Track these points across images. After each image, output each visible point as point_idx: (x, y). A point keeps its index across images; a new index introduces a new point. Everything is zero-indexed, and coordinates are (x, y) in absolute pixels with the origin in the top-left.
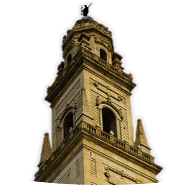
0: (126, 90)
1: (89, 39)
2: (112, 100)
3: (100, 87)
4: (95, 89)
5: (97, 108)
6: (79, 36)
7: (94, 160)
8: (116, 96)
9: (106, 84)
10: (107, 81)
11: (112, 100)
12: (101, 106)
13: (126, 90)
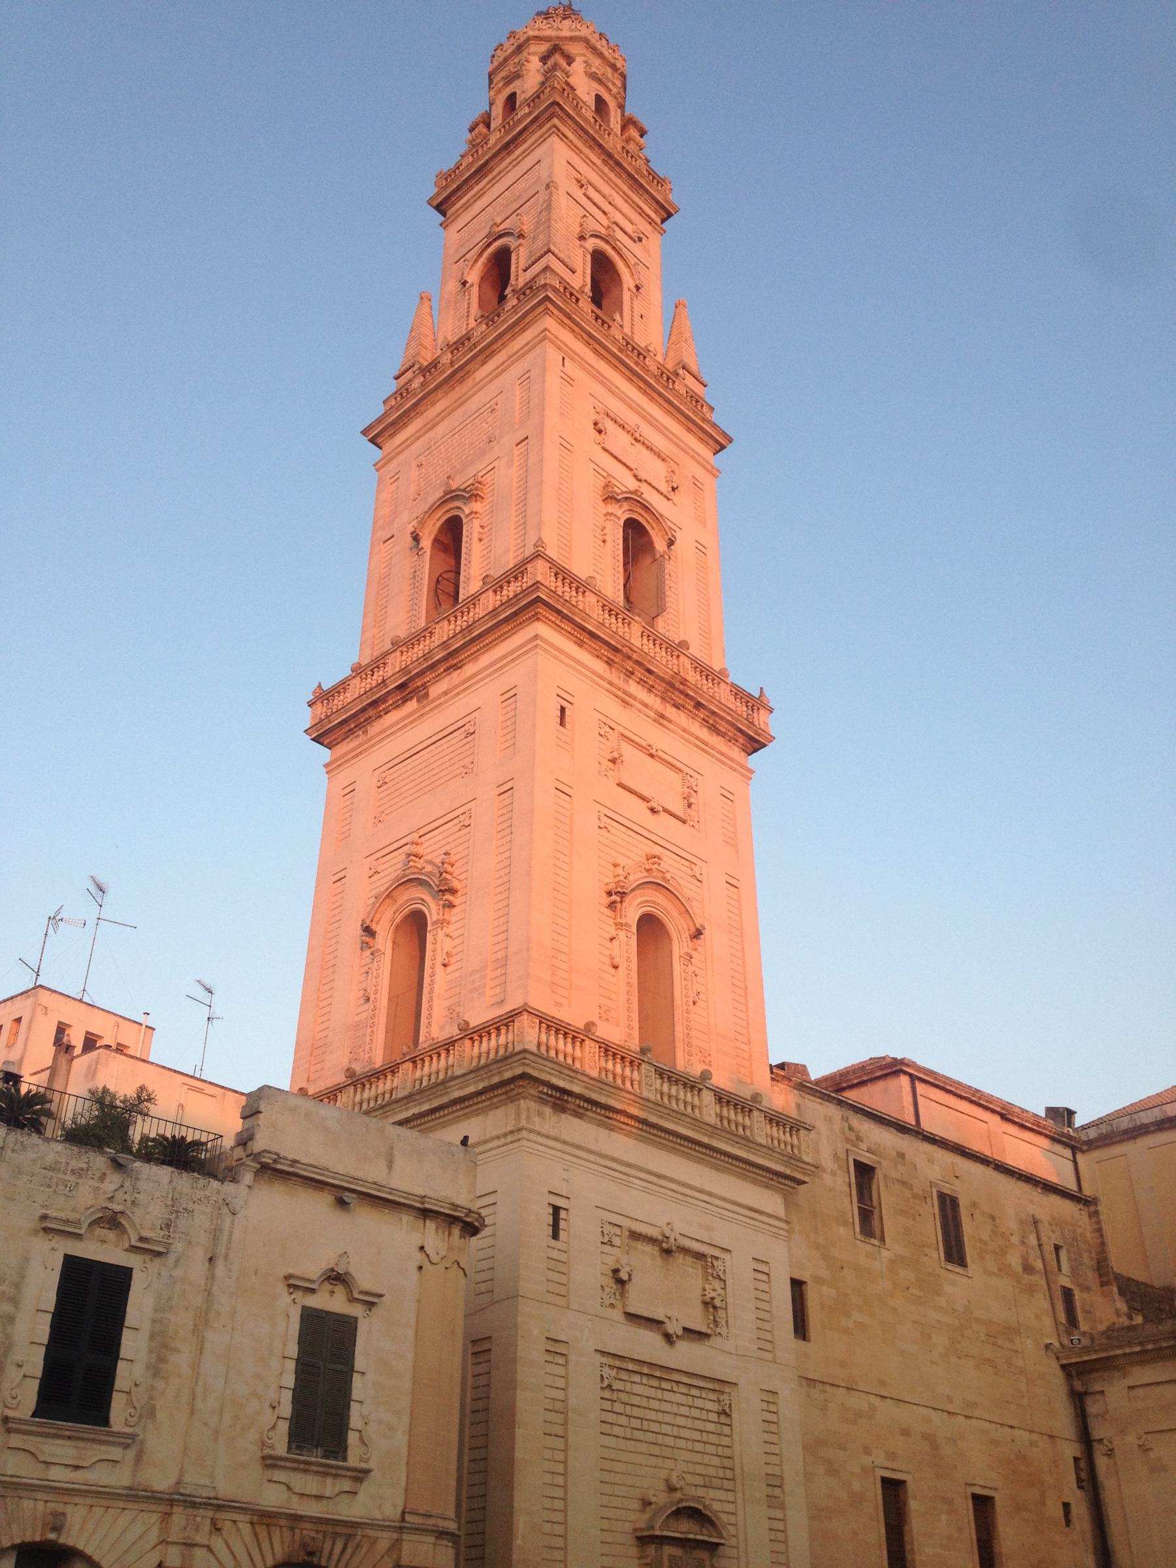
0: (653, 216)
1: (570, 60)
2: (619, 234)
3: (591, 192)
4: (579, 194)
5: (581, 246)
6: (543, 48)
7: (569, 380)
8: (629, 228)
9: (606, 190)
10: (609, 181)
11: (619, 234)
12: (591, 244)
13: (653, 216)
